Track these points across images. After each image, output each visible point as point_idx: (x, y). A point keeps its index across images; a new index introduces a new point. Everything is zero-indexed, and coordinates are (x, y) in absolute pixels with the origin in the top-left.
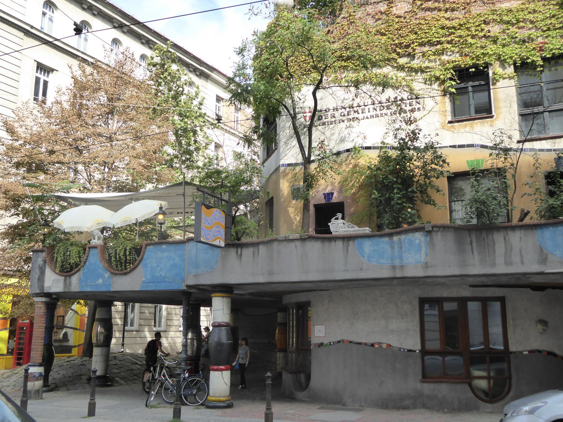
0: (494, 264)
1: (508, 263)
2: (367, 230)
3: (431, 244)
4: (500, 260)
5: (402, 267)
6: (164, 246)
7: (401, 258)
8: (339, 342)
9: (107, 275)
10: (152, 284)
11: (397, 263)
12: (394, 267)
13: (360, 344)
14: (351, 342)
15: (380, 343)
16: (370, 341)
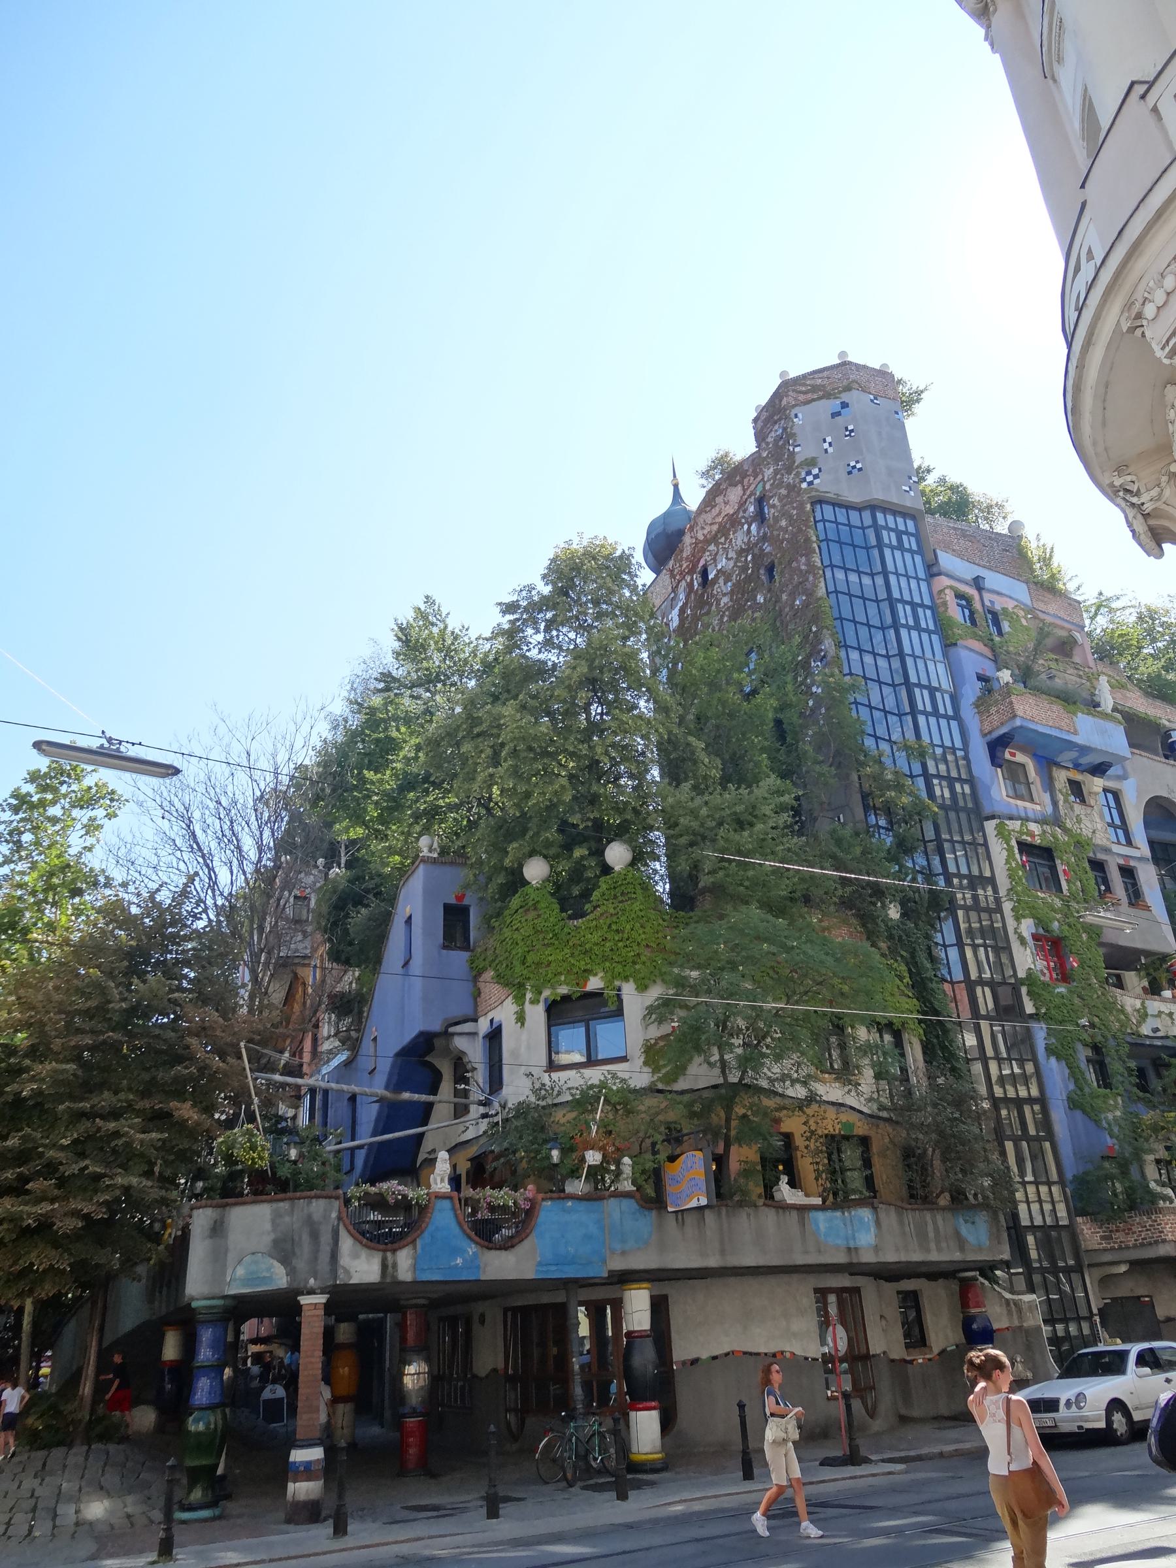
0: (928, 1251)
1: (939, 1250)
2: (818, 1201)
3: (878, 1223)
4: (933, 1245)
5: (856, 1249)
6: (570, 1204)
7: (854, 1239)
8: (727, 1354)
9: (472, 1249)
10: (553, 1268)
11: (852, 1245)
12: (849, 1249)
13: (758, 1354)
14: (745, 1353)
15: (782, 1352)
16: (772, 1348)
